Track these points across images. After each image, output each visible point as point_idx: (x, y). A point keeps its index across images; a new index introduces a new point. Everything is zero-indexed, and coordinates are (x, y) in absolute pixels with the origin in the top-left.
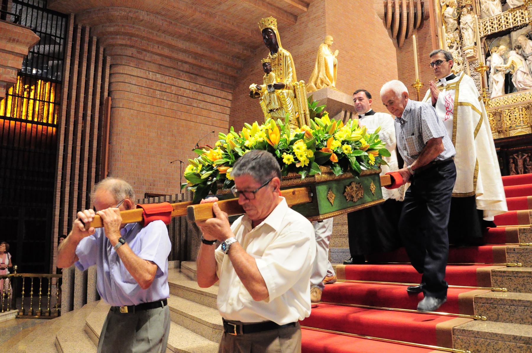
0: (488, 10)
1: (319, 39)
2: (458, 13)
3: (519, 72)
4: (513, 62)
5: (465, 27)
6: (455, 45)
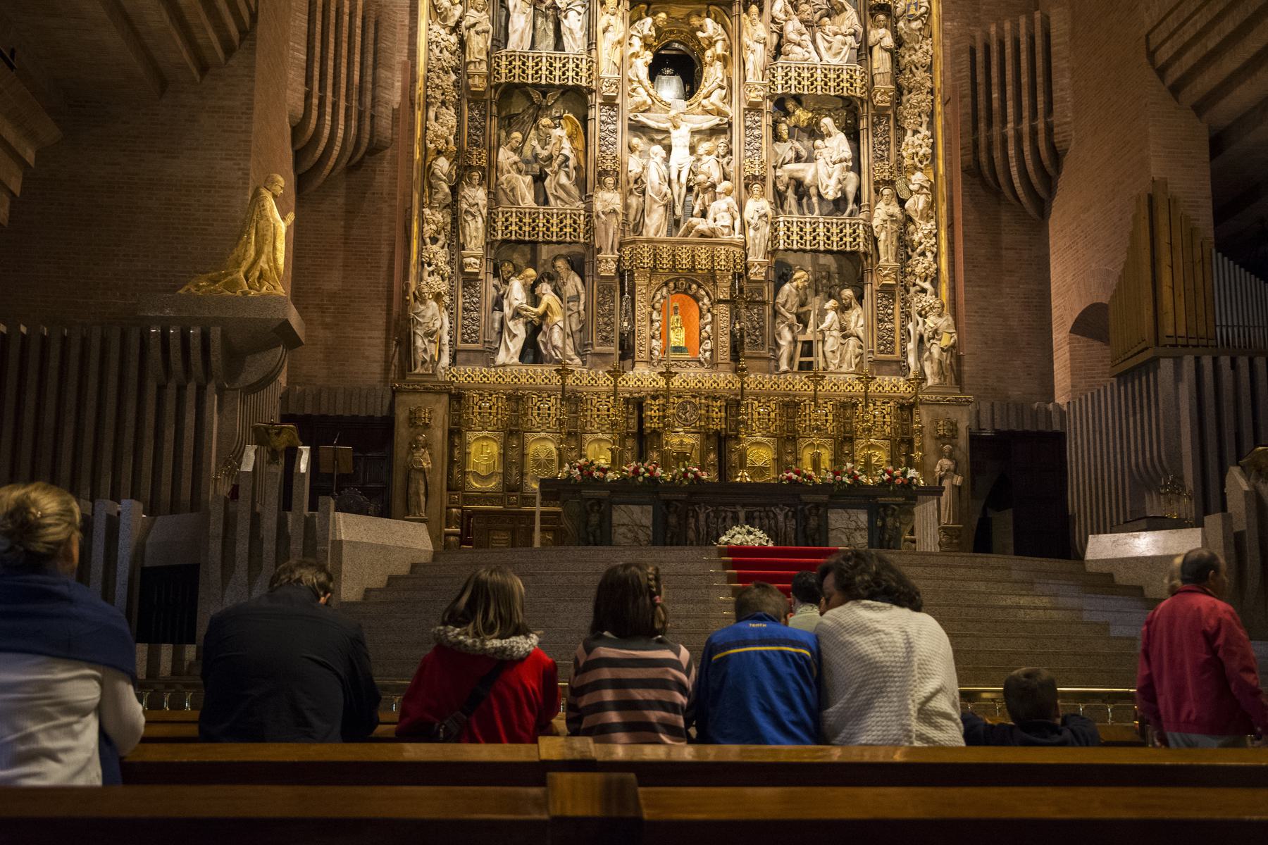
0: (513, 190)
1: (229, 163)
2: (457, 175)
3: (556, 329)
4: (548, 306)
5: (472, 210)
6: (442, 238)
